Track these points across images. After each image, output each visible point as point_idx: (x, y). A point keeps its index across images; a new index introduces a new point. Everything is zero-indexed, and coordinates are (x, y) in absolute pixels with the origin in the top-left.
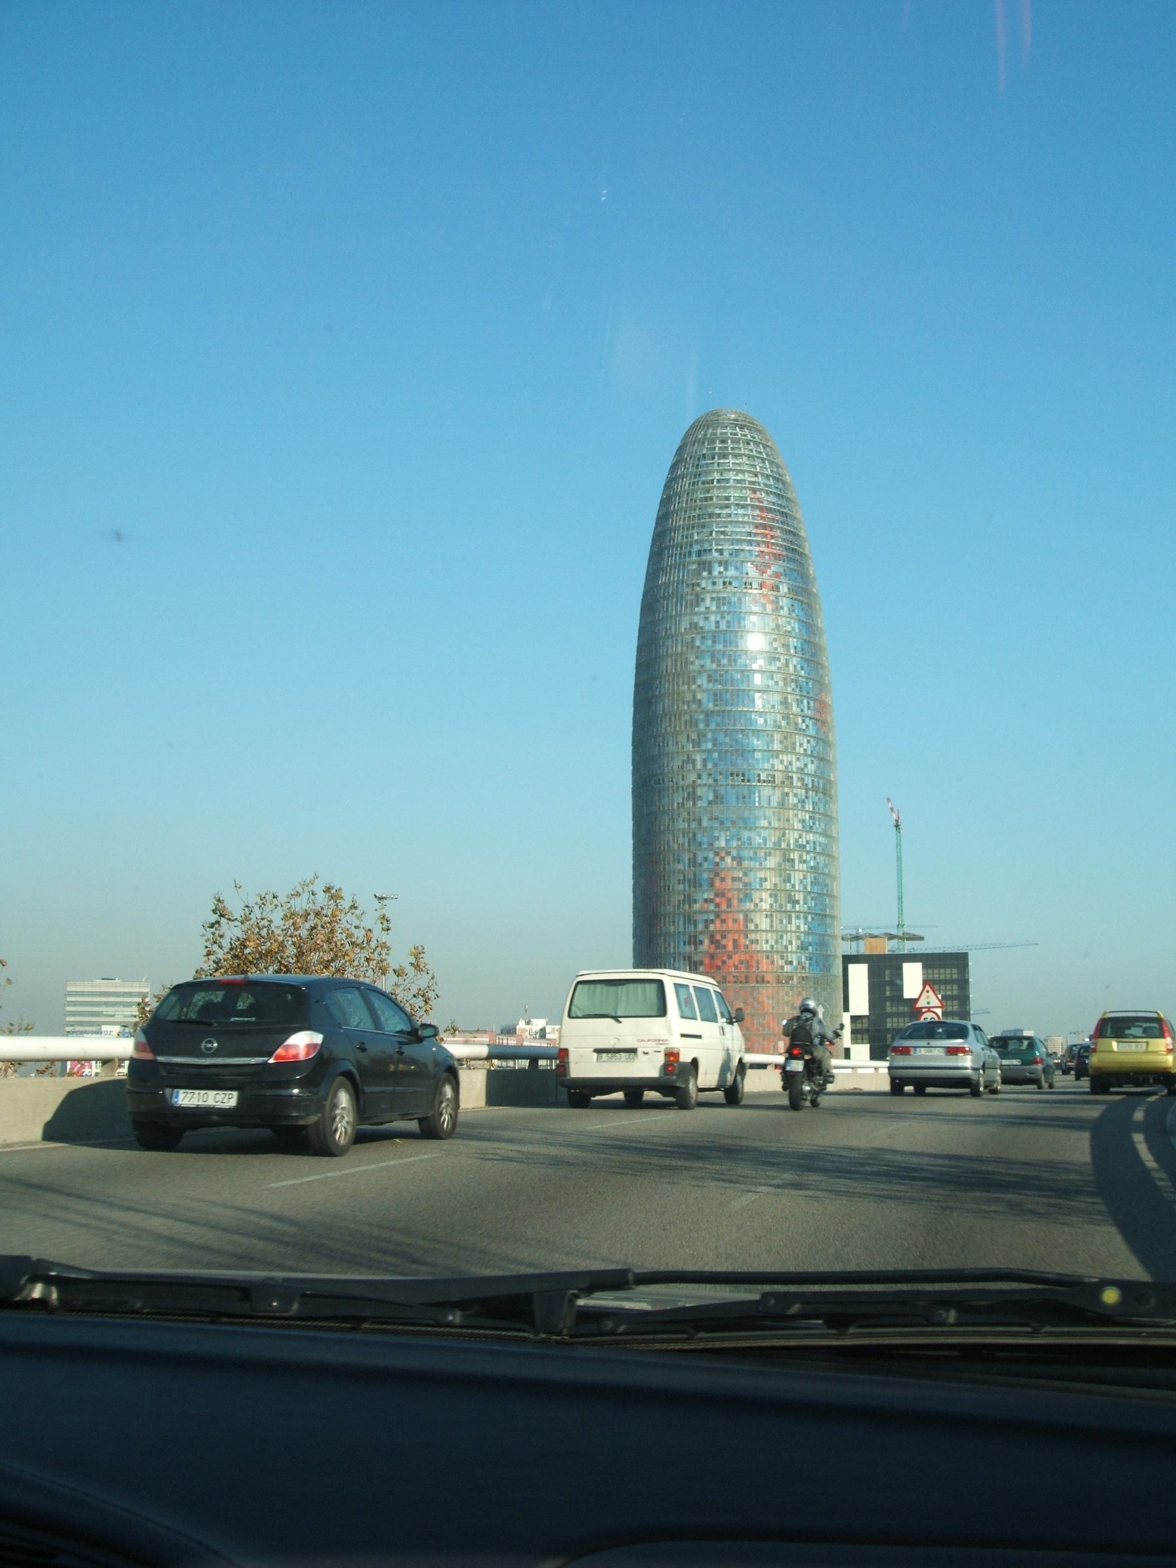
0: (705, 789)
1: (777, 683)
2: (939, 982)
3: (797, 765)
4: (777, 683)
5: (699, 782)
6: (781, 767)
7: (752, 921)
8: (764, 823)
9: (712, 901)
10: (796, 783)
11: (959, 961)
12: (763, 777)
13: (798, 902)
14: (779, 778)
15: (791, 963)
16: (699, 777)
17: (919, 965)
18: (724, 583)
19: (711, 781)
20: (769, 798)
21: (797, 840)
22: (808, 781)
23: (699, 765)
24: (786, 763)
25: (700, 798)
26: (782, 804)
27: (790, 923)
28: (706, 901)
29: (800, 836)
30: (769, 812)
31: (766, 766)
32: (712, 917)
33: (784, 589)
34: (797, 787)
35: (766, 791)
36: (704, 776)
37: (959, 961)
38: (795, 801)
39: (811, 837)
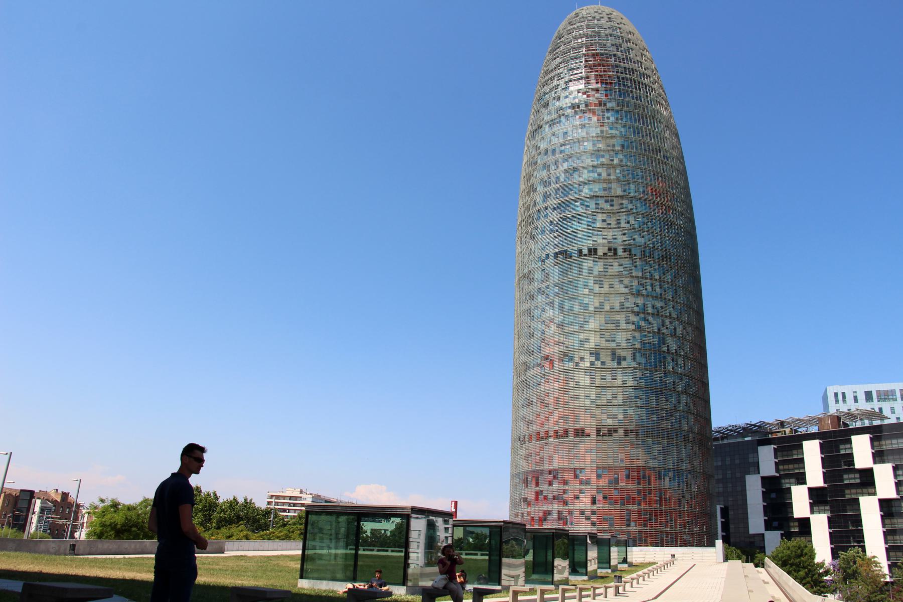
1: (599, 175)
3: (620, 238)
4: (599, 175)
6: (605, 241)
7: (572, 379)
10: (620, 252)
12: (585, 251)
13: (625, 358)
20: (590, 270)
21: (622, 304)
26: (604, 273)
27: (614, 378)
29: (627, 300)
30: (591, 283)
34: (621, 257)
35: (588, 263)
39: (640, 301)
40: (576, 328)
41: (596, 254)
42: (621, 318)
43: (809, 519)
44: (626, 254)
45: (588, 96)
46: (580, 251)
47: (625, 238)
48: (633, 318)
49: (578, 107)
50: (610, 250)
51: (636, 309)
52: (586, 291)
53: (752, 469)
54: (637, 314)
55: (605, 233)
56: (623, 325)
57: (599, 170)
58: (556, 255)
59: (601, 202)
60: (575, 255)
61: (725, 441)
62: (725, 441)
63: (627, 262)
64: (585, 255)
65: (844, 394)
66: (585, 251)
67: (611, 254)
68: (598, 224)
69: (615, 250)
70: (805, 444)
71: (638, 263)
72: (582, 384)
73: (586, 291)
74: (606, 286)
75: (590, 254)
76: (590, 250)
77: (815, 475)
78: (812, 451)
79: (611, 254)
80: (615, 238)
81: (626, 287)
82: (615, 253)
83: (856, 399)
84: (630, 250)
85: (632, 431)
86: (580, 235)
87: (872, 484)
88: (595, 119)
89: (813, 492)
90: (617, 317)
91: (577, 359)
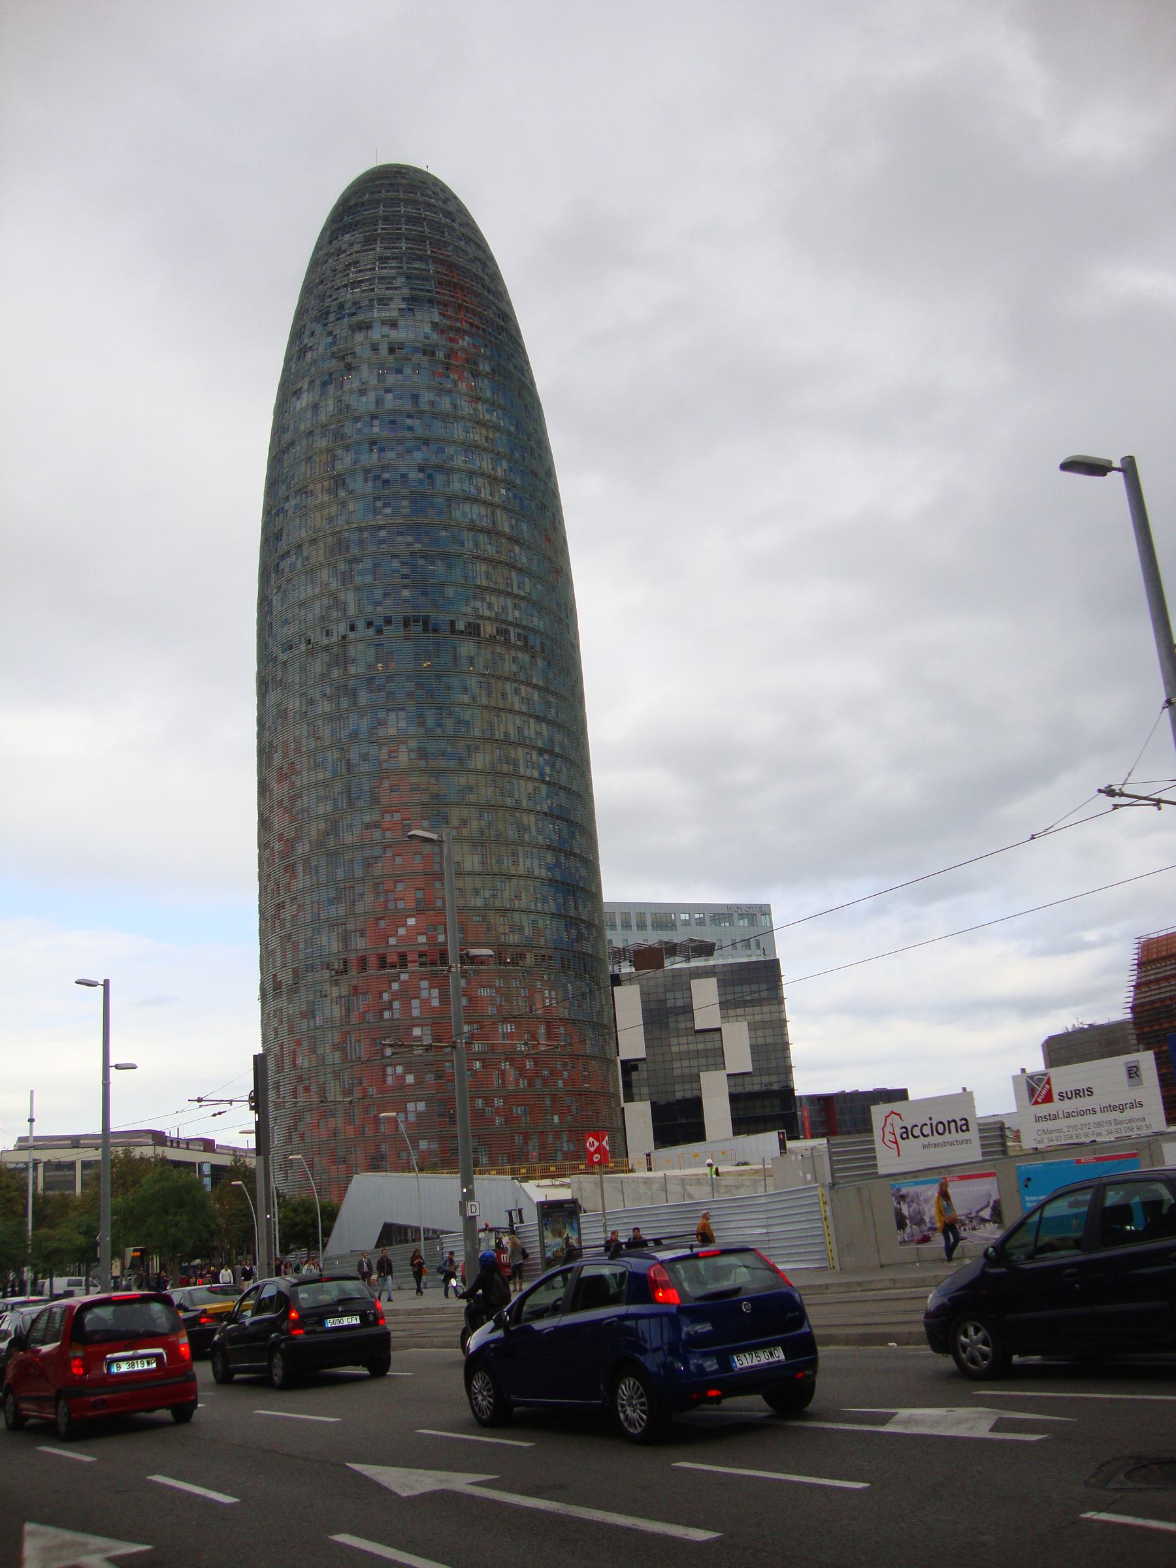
0: (361, 646)
2: (744, 1004)
5: (352, 635)
8: (466, 699)
9: (376, 825)
12: (461, 626)
14: (488, 629)
15: (521, 929)
16: (353, 628)
17: (714, 980)
18: (392, 351)
19: (371, 632)
23: (351, 611)
25: (354, 661)
27: (515, 863)
28: (367, 826)
32: (378, 851)
35: (467, 648)
36: (360, 625)
40: (452, 764)
41: (479, 634)
46: (453, 623)
49: (433, 354)
54: (541, 751)
57: (480, 481)
58: (407, 622)
63: (525, 657)
64: (462, 632)
66: (461, 626)
69: (506, 632)
71: (540, 662)
72: (467, 867)
73: (466, 699)
86: (450, 592)
91: (455, 822)
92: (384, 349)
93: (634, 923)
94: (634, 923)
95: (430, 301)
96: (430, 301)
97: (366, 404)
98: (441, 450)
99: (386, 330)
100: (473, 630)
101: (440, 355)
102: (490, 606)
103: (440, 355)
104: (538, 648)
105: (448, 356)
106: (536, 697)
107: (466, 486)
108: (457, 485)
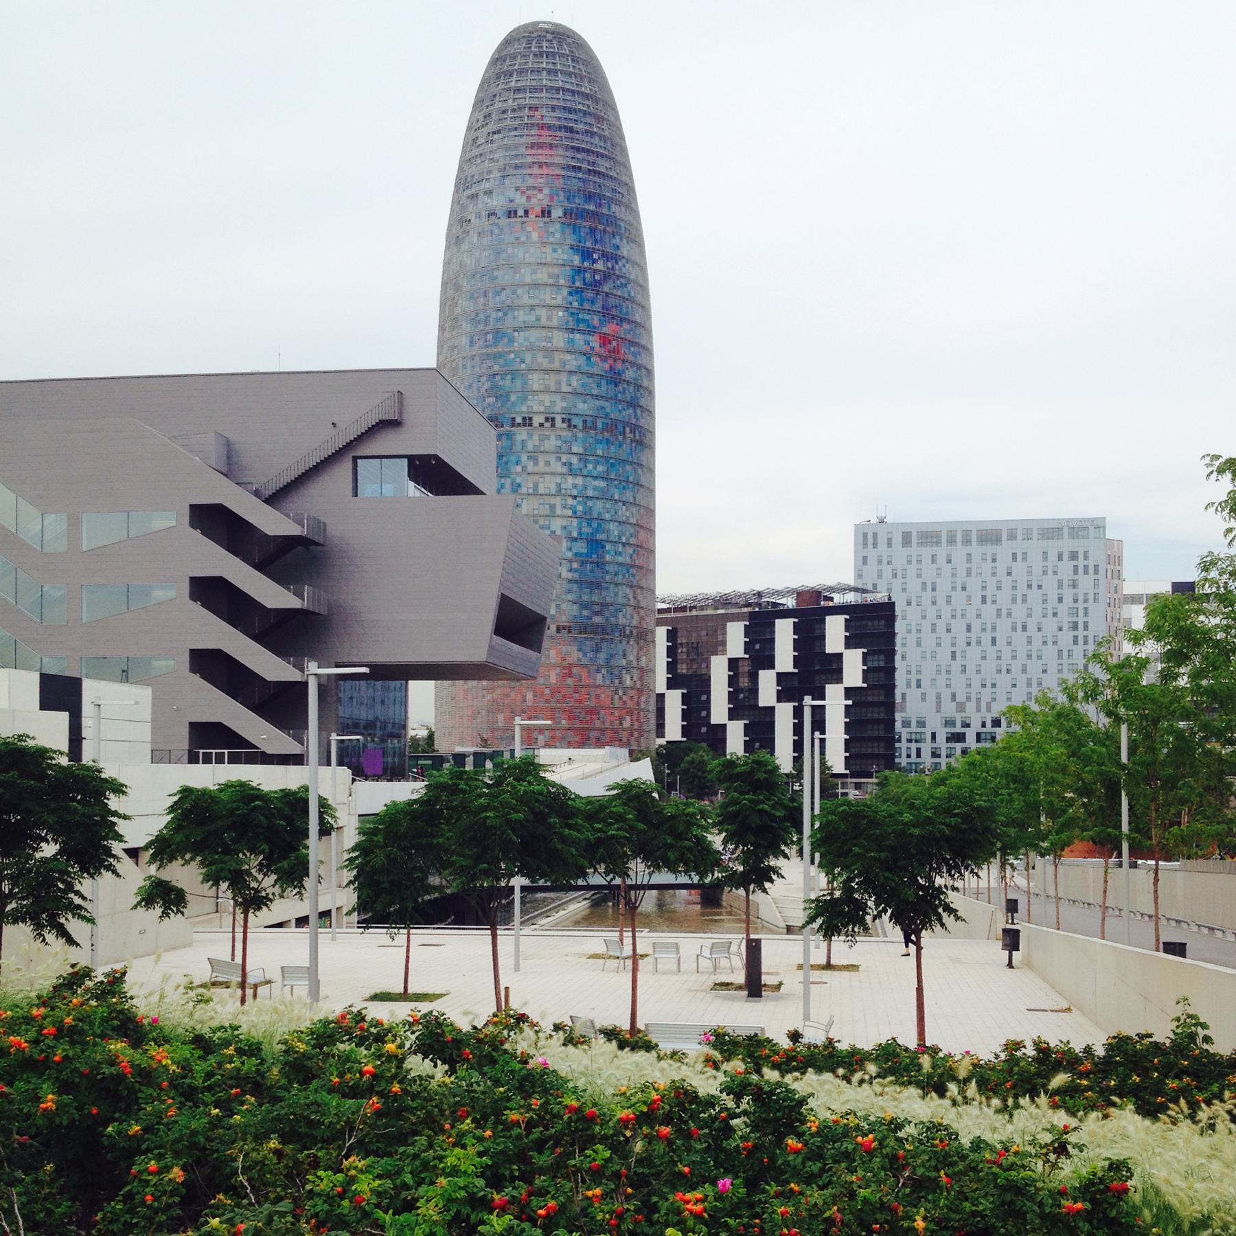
3: (560, 405)
4: (538, 319)
6: (542, 409)
11: (886, 611)
12: (519, 420)
21: (559, 485)
22: (576, 421)
24: (547, 403)
31: (524, 409)
33: (557, 213)
37: (886, 611)
38: (559, 443)
39: (579, 481)
41: (530, 425)
42: (557, 501)
43: (773, 708)
44: (565, 425)
45: (529, 198)
46: (513, 419)
47: (564, 404)
48: (570, 501)
49: (515, 212)
50: (547, 419)
51: (575, 492)
52: (519, 469)
53: (720, 648)
54: (575, 497)
55: (541, 397)
56: (559, 511)
59: (540, 355)
60: (507, 423)
61: (694, 613)
62: (694, 613)
63: (567, 434)
64: (519, 425)
65: (875, 535)
66: (519, 420)
67: (548, 425)
68: (536, 387)
69: (553, 419)
70: (779, 623)
73: (519, 469)
74: (541, 464)
75: (524, 425)
76: (524, 419)
77: (785, 658)
78: (784, 631)
79: (548, 425)
80: (553, 403)
81: (565, 464)
82: (553, 425)
83: (889, 545)
84: (569, 420)
85: (564, 628)
86: (513, 398)
87: (840, 671)
88: (535, 236)
89: (781, 677)
90: (553, 500)
92: (483, 213)
93: (959, 538)
94: (959, 538)
95: (517, 167)
96: (517, 167)
97: (470, 262)
98: (514, 292)
99: (486, 199)
100: (527, 421)
101: (521, 212)
102: (541, 403)
103: (521, 212)
104: (580, 425)
105: (526, 212)
106: (575, 460)
107: (527, 318)
108: (522, 316)
